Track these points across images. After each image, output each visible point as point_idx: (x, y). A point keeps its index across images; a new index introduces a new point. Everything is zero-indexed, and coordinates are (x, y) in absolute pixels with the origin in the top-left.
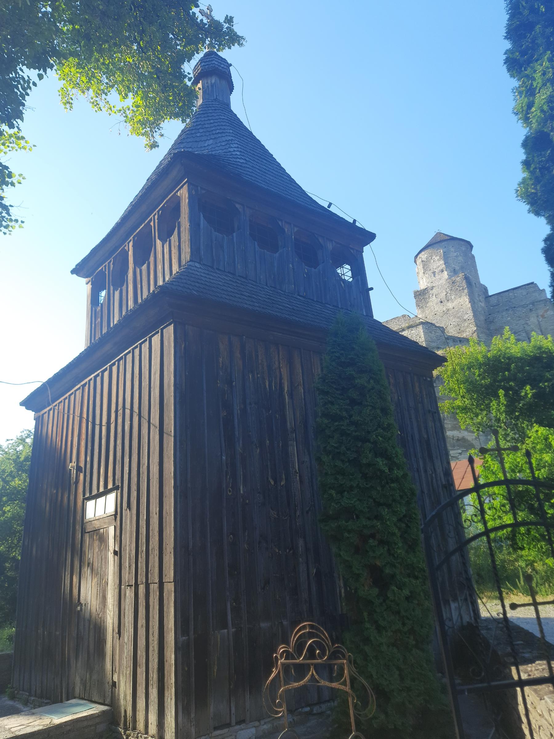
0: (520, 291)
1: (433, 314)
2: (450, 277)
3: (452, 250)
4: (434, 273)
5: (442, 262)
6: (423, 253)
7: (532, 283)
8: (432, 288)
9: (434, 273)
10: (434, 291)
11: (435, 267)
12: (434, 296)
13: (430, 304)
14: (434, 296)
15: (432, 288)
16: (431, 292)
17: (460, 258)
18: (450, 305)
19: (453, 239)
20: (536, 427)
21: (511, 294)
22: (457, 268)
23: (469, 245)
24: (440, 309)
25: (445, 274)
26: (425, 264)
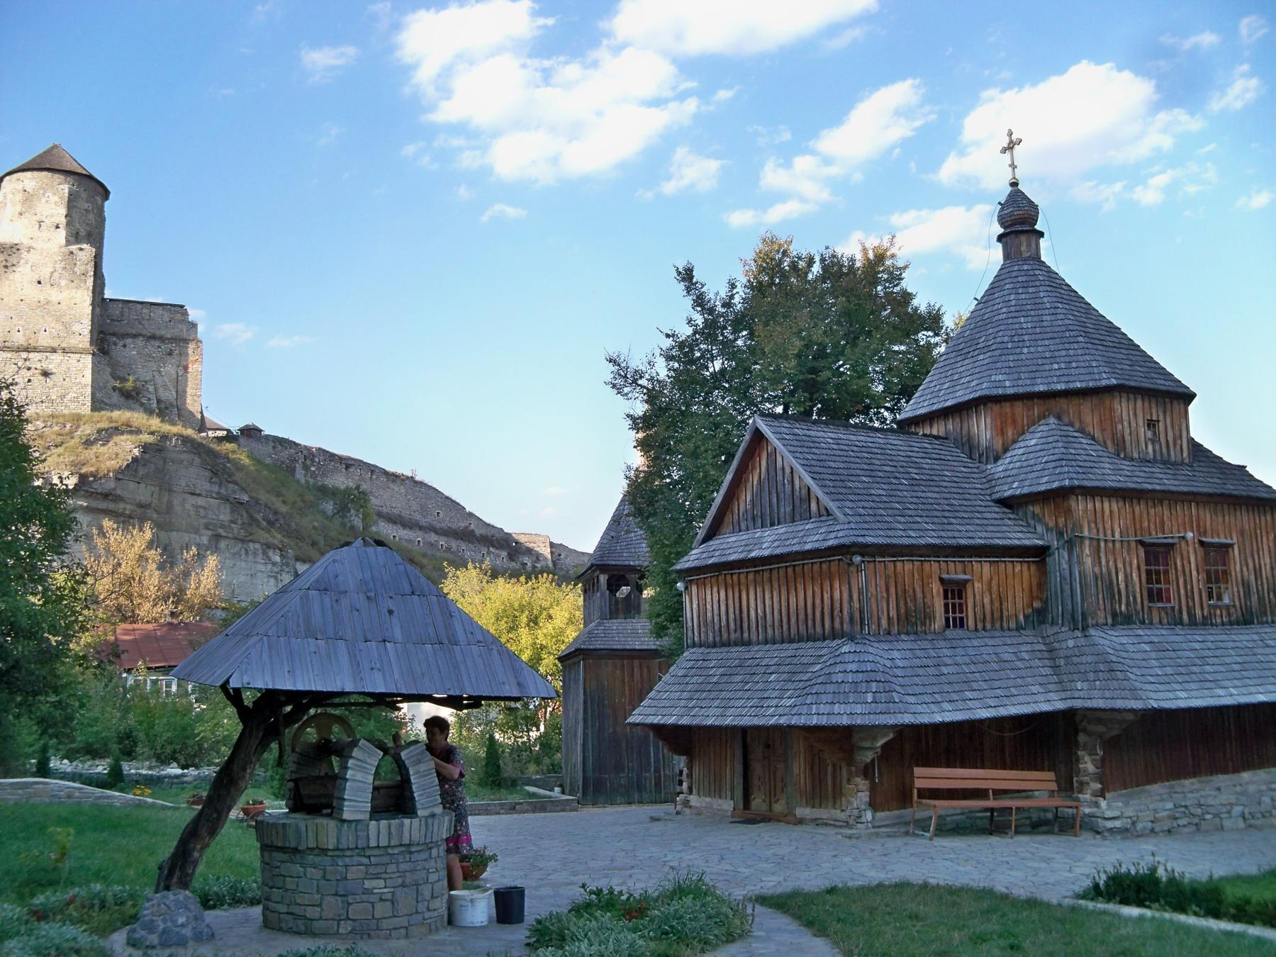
0: (160, 311)
1: (17, 297)
2: (68, 243)
3: (84, 195)
4: (40, 222)
5: (63, 211)
6: (29, 174)
7: (182, 307)
8: (29, 249)
9: (40, 222)
10: (32, 257)
11: (45, 214)
12: (29, 266)
13: (17, 277)
14: (29, 266)
15: (29, 249)
16: (24, 255)
17: (91, 216)
18: (54, 295)
19: (90, 177)
20: (575, 634)
21: (145, 311)
22: (83, 233)
23: (106, 194)
24: (32, 293)
25: (62, 235)
26: (28, 198)
